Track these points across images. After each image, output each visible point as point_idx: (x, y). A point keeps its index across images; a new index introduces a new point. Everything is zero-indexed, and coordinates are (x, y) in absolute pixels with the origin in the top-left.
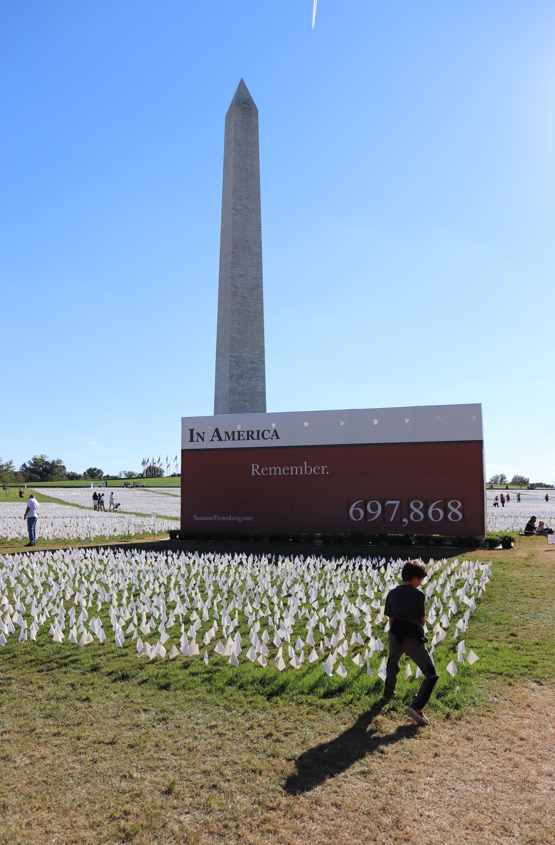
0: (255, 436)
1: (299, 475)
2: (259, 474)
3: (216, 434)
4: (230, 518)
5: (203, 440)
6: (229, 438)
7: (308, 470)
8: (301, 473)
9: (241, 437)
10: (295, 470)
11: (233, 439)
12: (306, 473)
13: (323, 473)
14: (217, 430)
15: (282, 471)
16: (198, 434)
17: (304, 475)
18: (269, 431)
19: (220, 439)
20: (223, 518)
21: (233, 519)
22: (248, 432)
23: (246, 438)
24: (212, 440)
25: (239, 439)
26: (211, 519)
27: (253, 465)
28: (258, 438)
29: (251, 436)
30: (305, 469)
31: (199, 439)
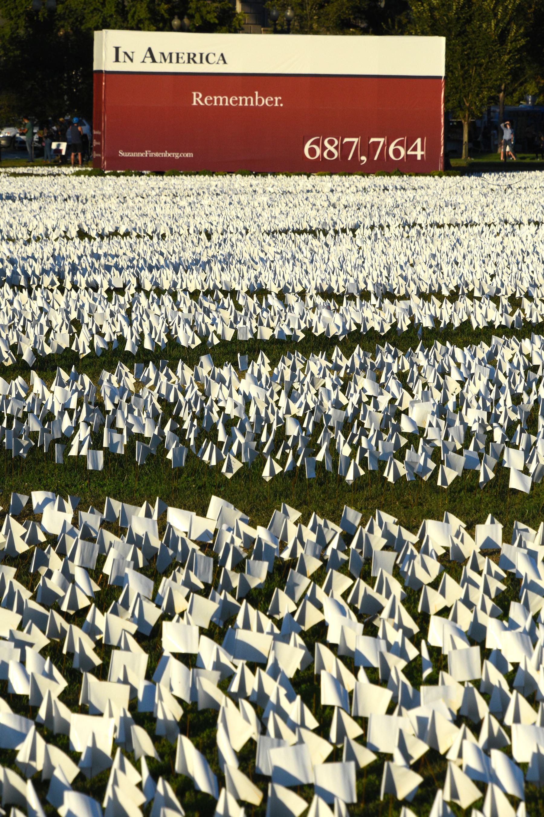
0: (197, 59)
2: (201, 104)
3: (148, 55)
4: (166, 154)
5: (132, 60)
7: (260, 101)
10: (244, 101)
11: (171, 62)
13: (276, 105)
14: (150, 50)
15: (230, 101)
16: (126, 53)
17: (255, 107)
19: (154, 61)
20: (157, 155)
21: (169, 155)
22: (189, 54)
25: (178, 62)
26: (142, 155)
27: (195, 93)
28: (201, 62)
30: (257, 100)
31: (127, 59)
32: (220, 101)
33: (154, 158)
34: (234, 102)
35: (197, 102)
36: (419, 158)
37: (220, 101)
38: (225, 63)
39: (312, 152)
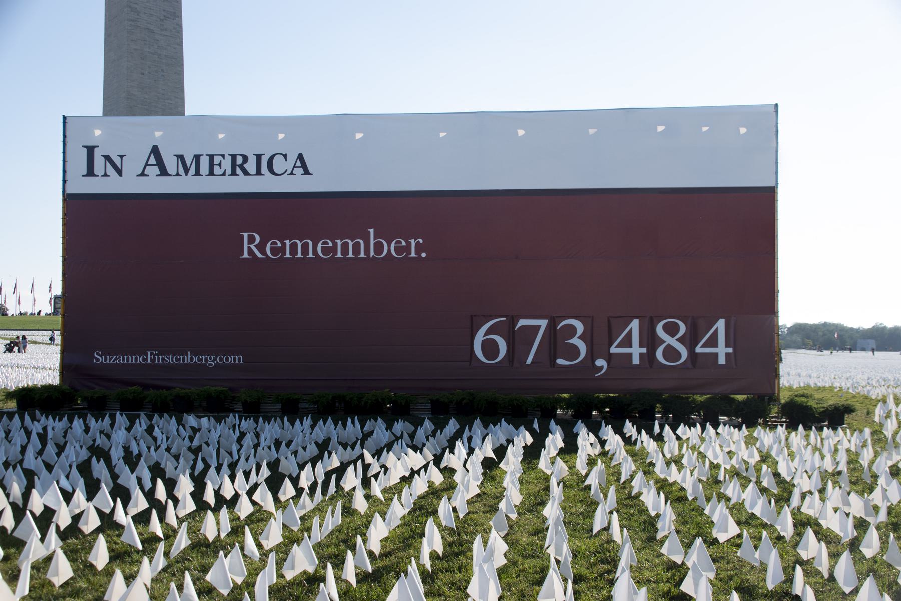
0: (251, 166)
1: (356, 259)
2: (260, 256)
3: (152, 160)
4: (187, 358)
5: (119, 172)
6: (187, 171)
7: (379, 248)
8: (362, 255)
9: (216, 168)
10: (346, 248)
11: (197, 173)
12: (372, 254)
13: (413, 255)
14: (155, 151)
15: (317, 249)
18: (285, 156)
19: (164, 172)
20: (171, 359)
21: (195, 359)
22: (234, 157)
23: (229, 172)
24: (143, 174)
25: (211, 173)
26: (140, 359)
27: (246, 235)
28: (259, 172)
29: (242, 167)
30: (372, 246)
31: (110, 170)
32: (295, 248)
33: (165, 367)
34: (325, 250)
35: (250, 251)
36: (722, 360)
37: (295, 248)
38: (307, 172)
39: (490, 348)
